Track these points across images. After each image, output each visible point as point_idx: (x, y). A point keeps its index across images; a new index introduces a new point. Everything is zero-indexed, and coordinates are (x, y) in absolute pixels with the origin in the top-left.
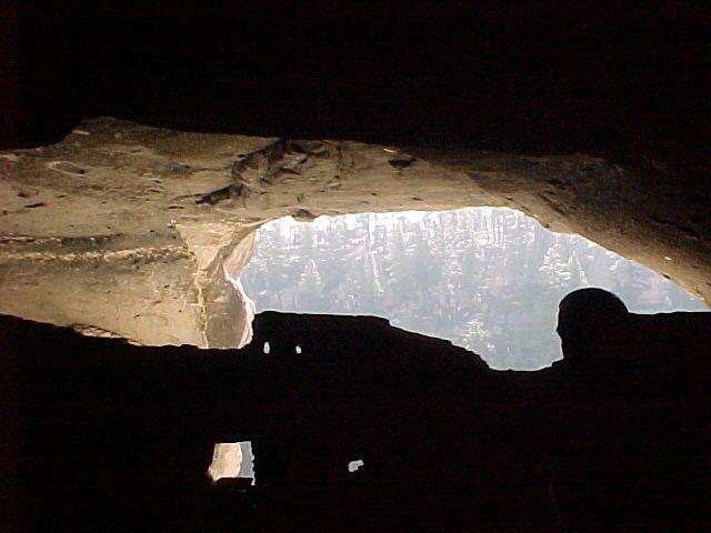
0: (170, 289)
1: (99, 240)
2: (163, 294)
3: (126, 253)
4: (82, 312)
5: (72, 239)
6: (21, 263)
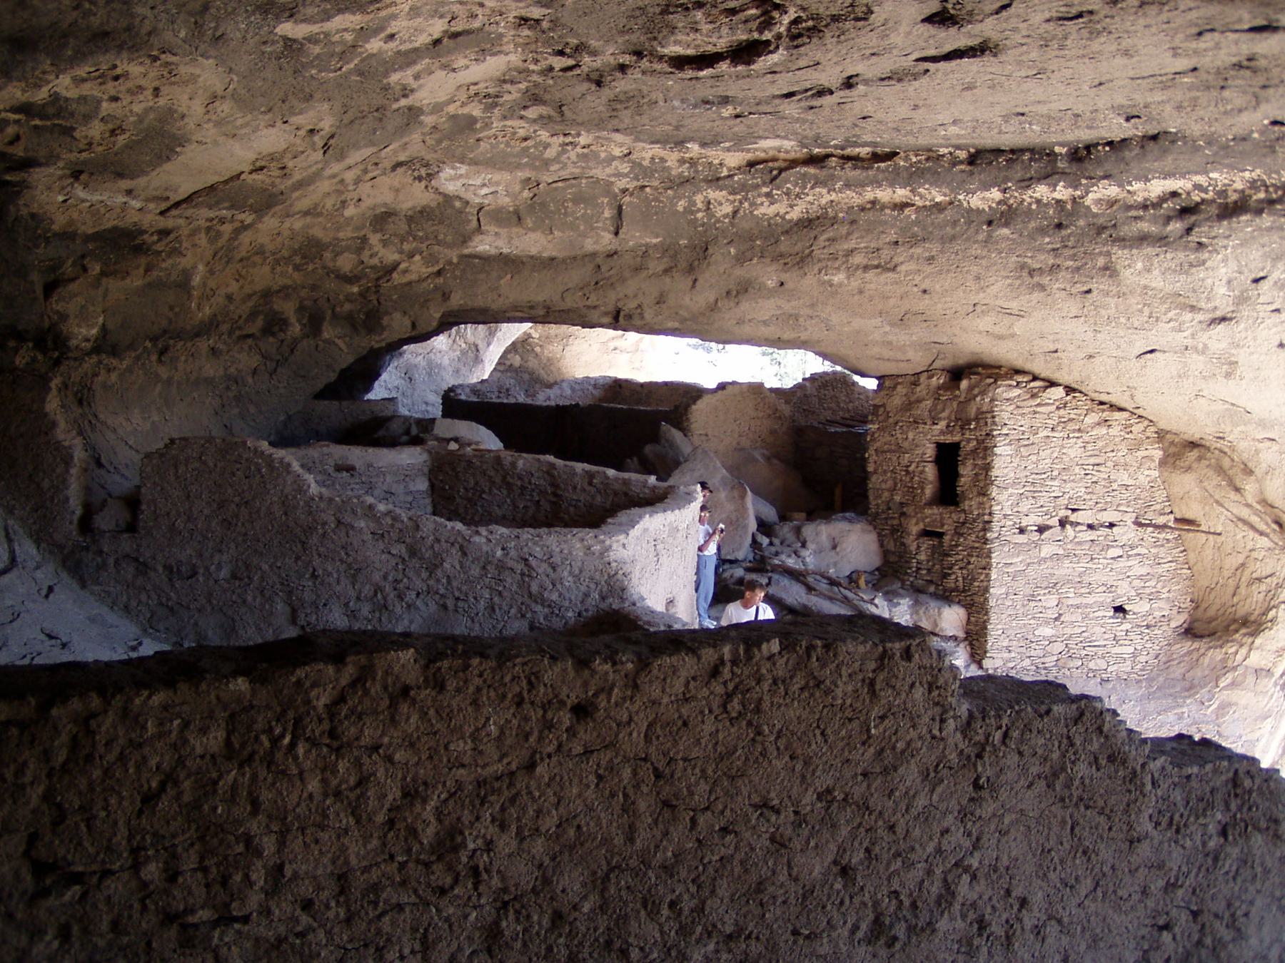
0: (1264, 285)
1: (1081, 155)
2: (1242, 300)
3: (1158, 187)
4: (1001, 337)
5: (998, 152)
6: (854, 218)
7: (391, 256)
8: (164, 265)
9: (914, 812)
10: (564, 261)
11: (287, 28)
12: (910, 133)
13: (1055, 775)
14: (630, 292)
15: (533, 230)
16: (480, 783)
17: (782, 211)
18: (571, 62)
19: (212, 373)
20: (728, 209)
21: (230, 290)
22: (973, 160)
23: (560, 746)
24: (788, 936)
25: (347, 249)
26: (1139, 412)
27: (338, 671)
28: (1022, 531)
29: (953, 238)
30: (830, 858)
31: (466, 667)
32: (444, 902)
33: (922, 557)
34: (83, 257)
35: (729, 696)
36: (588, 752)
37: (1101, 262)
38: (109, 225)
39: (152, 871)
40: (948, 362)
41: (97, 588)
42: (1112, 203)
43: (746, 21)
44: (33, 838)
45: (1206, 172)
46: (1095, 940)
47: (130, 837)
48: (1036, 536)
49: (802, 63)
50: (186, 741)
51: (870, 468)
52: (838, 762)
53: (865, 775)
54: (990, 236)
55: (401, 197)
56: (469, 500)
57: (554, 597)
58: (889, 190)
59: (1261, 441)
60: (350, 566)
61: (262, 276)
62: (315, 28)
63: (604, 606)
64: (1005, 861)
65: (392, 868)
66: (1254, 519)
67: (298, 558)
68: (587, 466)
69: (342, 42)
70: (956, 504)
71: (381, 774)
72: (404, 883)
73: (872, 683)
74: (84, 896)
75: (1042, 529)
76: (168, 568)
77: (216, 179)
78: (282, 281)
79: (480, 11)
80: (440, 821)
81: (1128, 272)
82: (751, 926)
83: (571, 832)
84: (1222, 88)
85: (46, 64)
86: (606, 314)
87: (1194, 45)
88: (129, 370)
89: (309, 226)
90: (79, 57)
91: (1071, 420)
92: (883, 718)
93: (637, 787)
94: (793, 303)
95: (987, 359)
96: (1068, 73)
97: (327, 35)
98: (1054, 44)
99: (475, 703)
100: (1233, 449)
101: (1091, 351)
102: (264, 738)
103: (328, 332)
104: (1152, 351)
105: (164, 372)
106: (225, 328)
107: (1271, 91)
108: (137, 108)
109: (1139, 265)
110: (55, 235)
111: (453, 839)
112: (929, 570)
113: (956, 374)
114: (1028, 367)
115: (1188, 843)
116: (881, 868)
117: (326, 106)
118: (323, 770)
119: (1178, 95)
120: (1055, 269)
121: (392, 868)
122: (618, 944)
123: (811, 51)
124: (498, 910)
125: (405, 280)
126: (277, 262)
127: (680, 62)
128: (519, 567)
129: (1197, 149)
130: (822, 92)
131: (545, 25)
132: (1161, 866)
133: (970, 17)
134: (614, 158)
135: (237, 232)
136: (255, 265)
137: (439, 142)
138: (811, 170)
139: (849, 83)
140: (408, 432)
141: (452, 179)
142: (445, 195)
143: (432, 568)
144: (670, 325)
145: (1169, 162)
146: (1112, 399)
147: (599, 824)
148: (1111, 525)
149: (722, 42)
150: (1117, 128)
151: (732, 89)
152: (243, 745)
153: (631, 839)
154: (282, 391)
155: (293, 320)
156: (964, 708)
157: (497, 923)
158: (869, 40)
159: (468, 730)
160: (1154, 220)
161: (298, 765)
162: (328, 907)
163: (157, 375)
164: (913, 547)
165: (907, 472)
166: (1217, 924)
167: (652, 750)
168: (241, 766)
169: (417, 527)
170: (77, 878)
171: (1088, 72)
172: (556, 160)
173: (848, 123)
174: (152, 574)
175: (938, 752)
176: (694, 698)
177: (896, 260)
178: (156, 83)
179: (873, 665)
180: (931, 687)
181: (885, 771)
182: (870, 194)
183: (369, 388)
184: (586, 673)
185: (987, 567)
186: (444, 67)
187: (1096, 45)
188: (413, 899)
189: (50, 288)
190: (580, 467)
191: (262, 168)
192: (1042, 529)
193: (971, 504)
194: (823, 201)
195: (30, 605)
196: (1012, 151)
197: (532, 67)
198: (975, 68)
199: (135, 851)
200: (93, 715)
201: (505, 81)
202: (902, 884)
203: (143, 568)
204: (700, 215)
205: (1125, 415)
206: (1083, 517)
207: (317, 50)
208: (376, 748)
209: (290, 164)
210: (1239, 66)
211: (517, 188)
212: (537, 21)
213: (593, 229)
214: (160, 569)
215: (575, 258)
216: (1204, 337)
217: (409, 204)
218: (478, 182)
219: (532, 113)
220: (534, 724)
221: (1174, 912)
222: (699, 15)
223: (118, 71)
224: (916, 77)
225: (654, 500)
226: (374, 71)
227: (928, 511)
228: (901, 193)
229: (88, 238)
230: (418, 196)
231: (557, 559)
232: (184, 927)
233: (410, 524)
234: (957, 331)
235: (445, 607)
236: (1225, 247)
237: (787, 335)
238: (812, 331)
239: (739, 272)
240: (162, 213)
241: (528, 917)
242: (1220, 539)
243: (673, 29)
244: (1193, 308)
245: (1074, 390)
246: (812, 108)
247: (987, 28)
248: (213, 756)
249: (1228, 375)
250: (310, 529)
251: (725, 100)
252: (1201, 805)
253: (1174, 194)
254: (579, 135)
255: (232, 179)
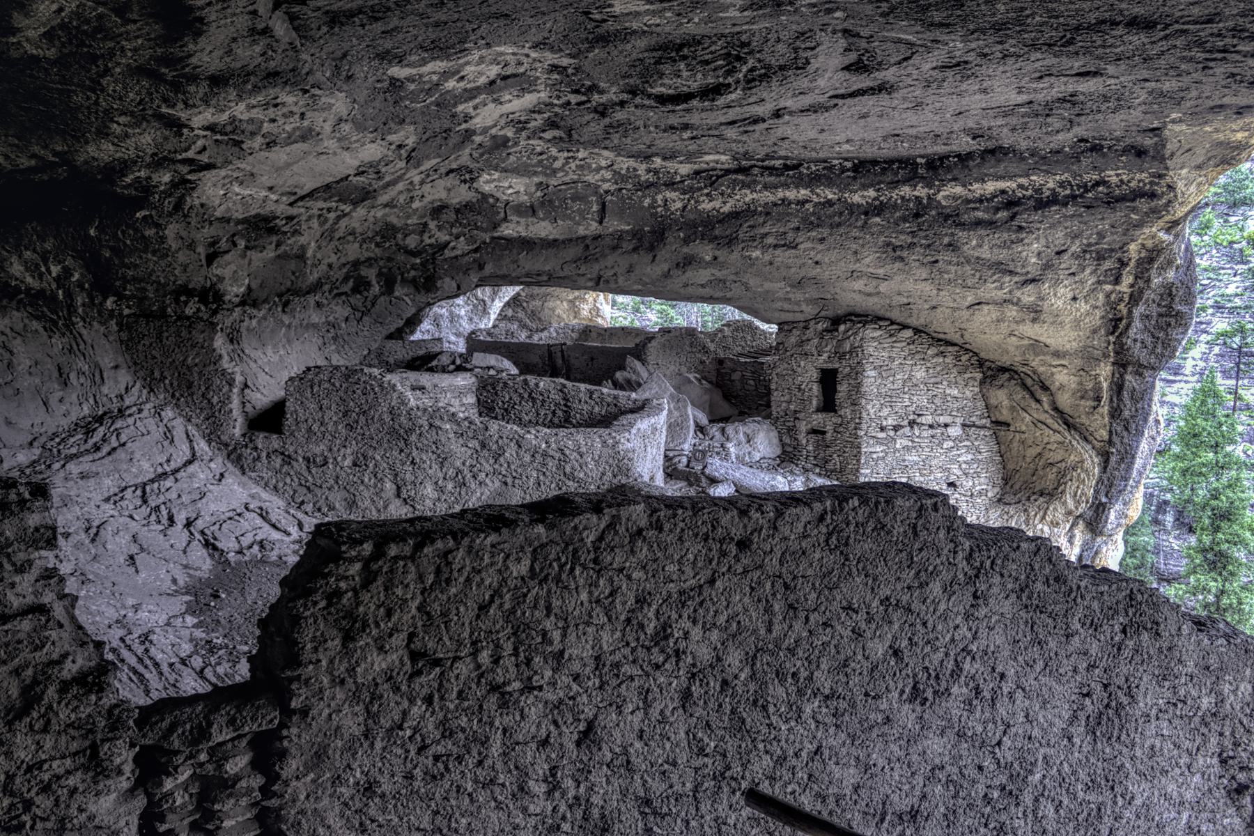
0: (1066, 256)
2: (1047, 266)
3: (991, 187)
4: (869, 295)
5: (875, 162)
7: (443, 237)
8: (289, 242)
9: (938, 613)
10: (563, 242)
11: (397, 71)
12: (814, 149)
13: (1022, 590)
14: (609, 264)
15: (543, 220)
16: (682, 593)
17: (718, 206)
18: (584, 98)
19: (317, 320)
20: (679, 205)
21: (330, 260)
22: (856, 168)
23: (730, 567)
24: (861, 697)
25: (413, 232)
26: (967, 346)
27: (600, 519)
28: (882, 429)
29: (839, 225)
30: (888, 644)
31: (675, 516)
32: (658, 674)
33: (811, 448)
34: (234, 235)
35: (830, 535)
36: (745, 572)
37: (946, 240)
38: (253, 213)
39: (485, 657)
40: (830, 313)
41: (253, 475)
42: (955, 198)
43: (715, 70)
44: (411, 636)
45: (1028, 176)
46: (1045, 702)
47: (472, 634)
48: (892, 433)
49: (752, 100)
50: (508, 568)
51: (773, 386)
52: (893, 580)
53: (909, 588)
54: (866, 223)
55: (452, 194)
56: (506, 410)
57: (582, 475)
58: (795, 191)
59: (1055, 367)
60: (439, 456)
61: (353, 251)
62: (414, 71)
63: (615, 481)
64: (992, 648)
65: (627, 651)
66: (1050, 421)
67: (402, 451)
68: (589, 387)
69: (430, 81)
70: (835, 411)
71: (624, 587)
72: (634, 662)
73: (915, 527)
74: (442, 673)
75: (896, 428)
76: (307, 459)
77: (331, 179)
78: (367, 254)
79: (525, 60)
80: (658, 619)
81: (966, 247)
82: (840, 690)
83: (734, 625)
84: (1048, 115)
85: (233, 94)
86: (591, 280)
87: (1035, 85)
88: (265, 318)
89: (386, 215)
90: (257, 89)
91: (918, 352)
92: (921, 550)
93: (774, 595)
94: (724, 272)
95: (858, 310)
96: (938, 105)
97: (421, 76)
98: (935, 85)
99: (680, 539)
100: (1035, 372)
101: (934, 303)
102: (555, 564)
103: (399, 291)
104: (979, 304)
105: (286, 319)
106: (326, 287)
107: (1083, 118)
108: (288, 128)
109: (974, 242)
110: (217, 219)
111: (665, 631)
112: (815, 457)
113: (836, 321)
114: (888, 315)
115: (1102, 638)
116: (919, 651)
117: (412, 128)
118: (590, 585)
119: (1014, 121)
120: (911, 246)
121: (627, 651)
122: (760, 703)
123: (761, 91)
124: (689, 679)
125: (453, 255)
126: (364, 241)
127: (662, 100)
128: (557, 455)
129: (1023, 159)
130: (757, 120)
131: (570, 71)
132: (1085, 654)
133: (880, 66)
134: (601, 168)
135: (339, 218)
136: (348, 242)
137: (482, 155)
138: (740, 177)
139: (777, 114)
140: (453, 363)
141: (487, 182)
142: (483, 194)
143: (497, 456)
144: (635, 287)
145: (1001, 169)
146: (948, 337)
147: (751, 620)
148: (946, 426)
149: (694, 86)
150: (964, 144)
151: (695, 119)
152: (542, 570)
153: (770, 631)
154: (366, 333)
155: (374, 282)
156: (967, 545)
157: (689, 688)
158: (804, 83)
159: (676, 557)
160: (986, 210)
161: (576, 582)
162: (589, 678)
163: (282, 321)
164: (804, 442)
165: (800, 389)
166: (1119, 693)
167: (784, 570)
168: (540, 583)
169: (487, 429)
170: (437, 662)
171: (952, 104)
172: (562, 169)
173: (769, 143)
174: (294, 463)
175: (952, 574)
176: (809, 535)
177: (798, 240)
178: (303, 110)
179: (914, 515)
180: (949, 529)
181: (921, 586)
182: (780, 194)
183: (412, 332)
184: (746, 520)
185: (857, 455)
186: (494, 100)
187: (964, 86)
188: (640, 672)
189: (211, 259)
190: (583, 387)
191: (363, 172)
192: (896, 428)
193: (846, 412)
194: (747, 199)
195: (211, 487)
196: (885, 162)
197: (556, 102)
198: (871, 103)
199: (474, 643)
200: (451, 551)
201: (534, 112)
202: (930, 661)
203: (288, 459)
204: (659, 209)
205: (957, 348)
206: (928, 419)
207: (412, 87)
208: (621, 570)
209: (383, 170)
210: (1064, 100)
211: (533, 189)
212: (565, 68)
213: (585, 219)
214: (301, 460)
215: (571, 240)
216: (1018, 294)
217: (457, 200)
218: (507, 184)
219: (548, 135)
220: (715, 554)
221: (1093, 685)
222: (682, 66)
223: (279, 101)
224: (827, 109)
225: (640, 408)
226: (446, 103)
227: (815, 416)
228: (804, 193)
229: (239, 222)
230: (463, 194)
231: (584, 449)
232: (503, 694)
233: (481, 426)
234: (838, 291)
235: (506, 484)
236: (1038, 229)
237: (719, 294)
238: (737, 290)
239: (685, 250)
240: (291, 204)
241: (708, 684)
242: (1023, 436)
243: (662, 75)
244: (1011, 273)
245: (920, 331)
246: (746, 132)
247: (889, 75)
248: (523, 578)
249: (1034, 320)
250: (409, 431)
251: (686, 127)
252: (1111, 612)
253: (1003, 192)
254: (578, 151)
255: (342, 180)
